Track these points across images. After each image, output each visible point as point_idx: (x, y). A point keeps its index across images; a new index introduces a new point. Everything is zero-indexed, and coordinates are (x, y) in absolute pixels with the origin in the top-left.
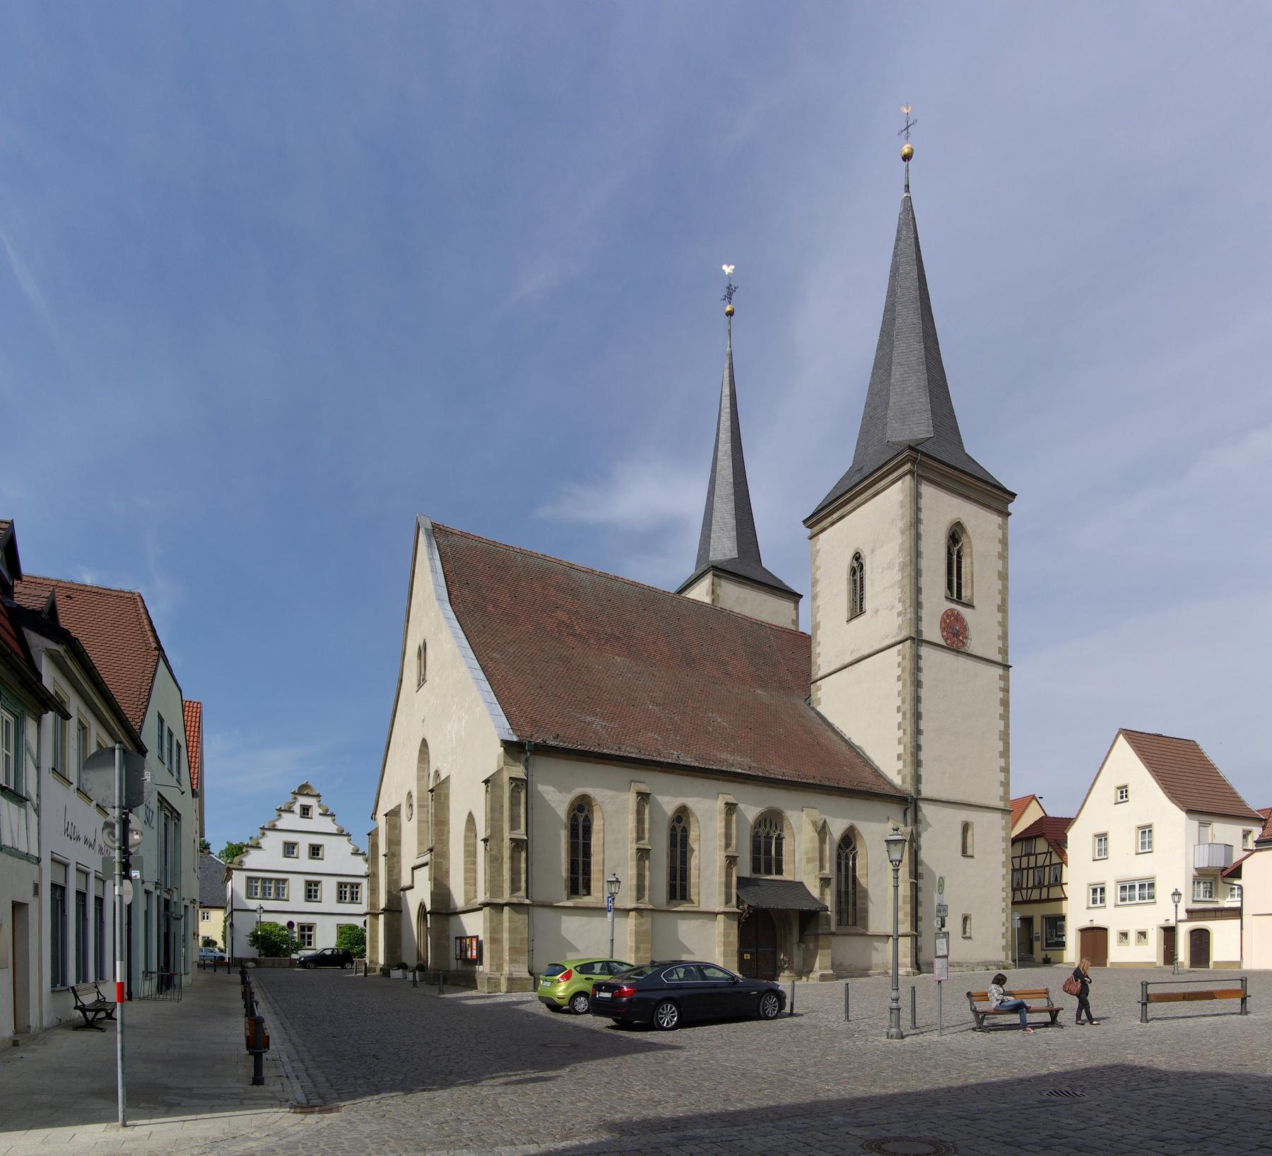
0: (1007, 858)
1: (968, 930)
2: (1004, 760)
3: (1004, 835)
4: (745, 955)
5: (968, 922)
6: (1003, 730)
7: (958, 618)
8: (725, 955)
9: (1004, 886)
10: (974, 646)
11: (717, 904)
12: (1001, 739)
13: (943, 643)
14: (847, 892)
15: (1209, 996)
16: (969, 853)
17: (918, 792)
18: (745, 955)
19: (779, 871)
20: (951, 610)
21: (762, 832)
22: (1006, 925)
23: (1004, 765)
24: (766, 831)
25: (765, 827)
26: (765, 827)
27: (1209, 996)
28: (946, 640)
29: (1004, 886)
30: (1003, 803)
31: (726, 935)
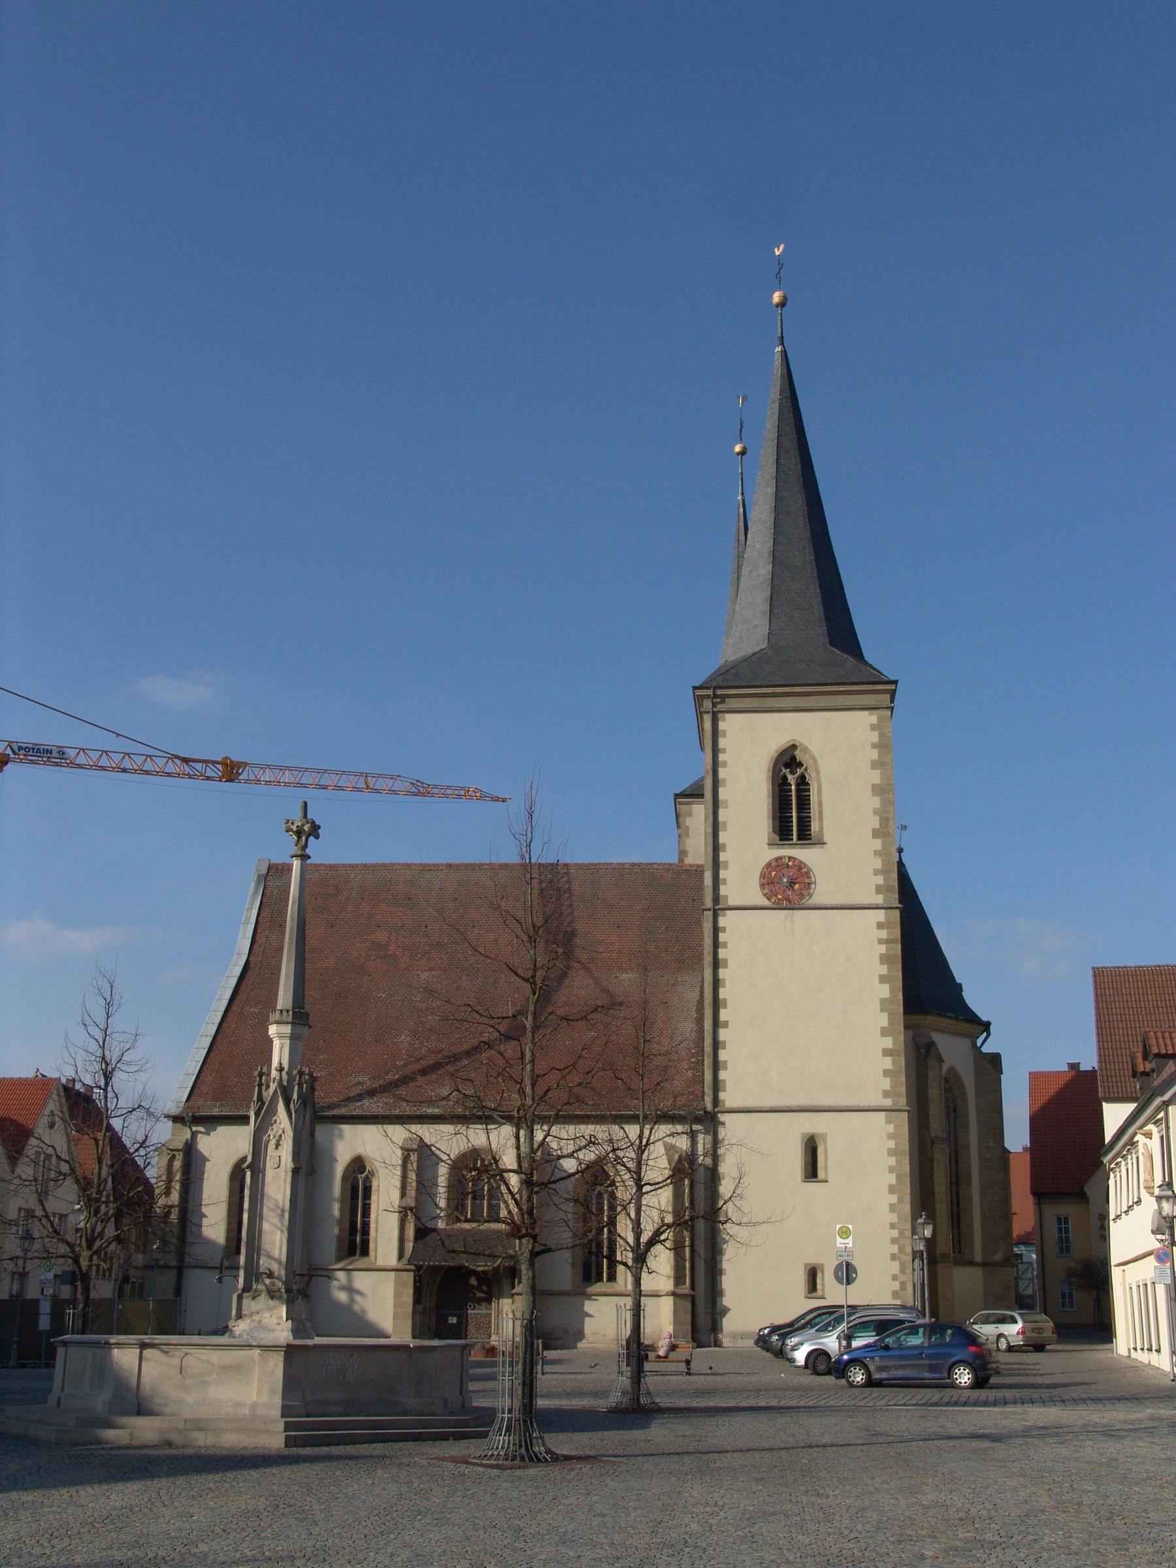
0: (898, 1178)
1: (819, 1287)
2: (891, 1038)
3: (894, 1147)
4: (450, 1318)
5: (819, 1275)
8: (396, 1316)
9: (896, 1221)
10: (822, 893)
11: (392, 1260)
13: (766, 903)
16: (821, 1174)
17: (716, 1101)
18: (450, 1318)
20: (778, 859)
22: (902, 1278)
23: (891, 1047)
28: (769, 899)
29: (896, 1221)
30: (891, 1100)
31: (397, 1295)
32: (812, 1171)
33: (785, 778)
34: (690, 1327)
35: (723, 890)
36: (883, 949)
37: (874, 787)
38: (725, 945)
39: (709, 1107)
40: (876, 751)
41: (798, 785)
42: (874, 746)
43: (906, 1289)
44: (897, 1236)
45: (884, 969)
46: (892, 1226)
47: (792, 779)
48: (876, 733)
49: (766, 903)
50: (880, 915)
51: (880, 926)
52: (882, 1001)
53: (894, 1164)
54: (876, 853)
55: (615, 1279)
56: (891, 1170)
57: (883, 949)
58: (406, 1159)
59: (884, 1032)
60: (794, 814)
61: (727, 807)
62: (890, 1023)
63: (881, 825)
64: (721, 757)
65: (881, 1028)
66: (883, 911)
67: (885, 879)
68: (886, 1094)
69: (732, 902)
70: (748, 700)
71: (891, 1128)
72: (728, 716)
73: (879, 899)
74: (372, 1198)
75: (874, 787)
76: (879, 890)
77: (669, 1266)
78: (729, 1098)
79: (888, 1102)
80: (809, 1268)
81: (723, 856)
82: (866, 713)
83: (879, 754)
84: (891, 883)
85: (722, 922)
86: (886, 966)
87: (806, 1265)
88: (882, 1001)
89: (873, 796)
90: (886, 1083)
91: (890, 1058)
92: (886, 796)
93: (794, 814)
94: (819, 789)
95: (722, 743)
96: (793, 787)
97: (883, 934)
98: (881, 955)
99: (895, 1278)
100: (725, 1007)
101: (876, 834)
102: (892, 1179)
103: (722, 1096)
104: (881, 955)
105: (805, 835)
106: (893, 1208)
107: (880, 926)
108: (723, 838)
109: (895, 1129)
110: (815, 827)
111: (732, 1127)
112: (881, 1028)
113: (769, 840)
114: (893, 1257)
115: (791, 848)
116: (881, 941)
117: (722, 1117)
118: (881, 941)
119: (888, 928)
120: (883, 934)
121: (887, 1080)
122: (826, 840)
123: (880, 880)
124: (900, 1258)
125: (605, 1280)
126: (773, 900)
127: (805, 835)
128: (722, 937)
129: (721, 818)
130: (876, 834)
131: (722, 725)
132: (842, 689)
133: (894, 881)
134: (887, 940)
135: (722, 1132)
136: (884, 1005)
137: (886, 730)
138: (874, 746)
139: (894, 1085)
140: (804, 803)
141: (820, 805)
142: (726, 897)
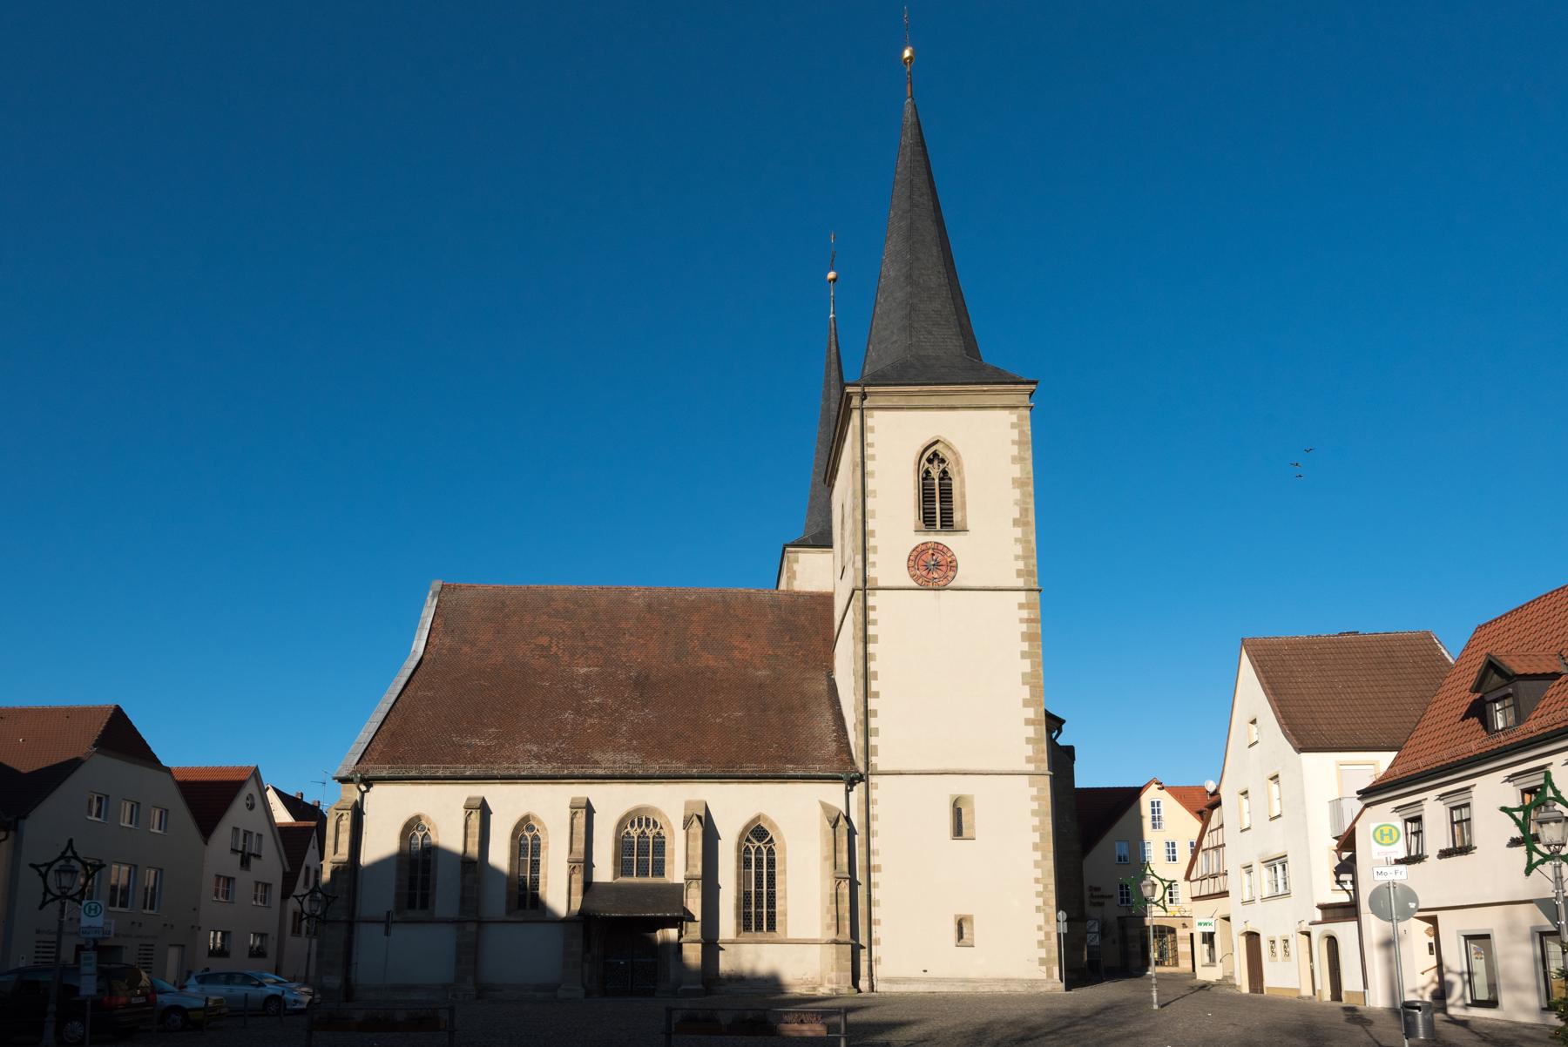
0: (1042, 837)
1: (965, 936)
2: (1032, 709)
6: (1029, 670)
7: (938, 548)
9: (1040, 876)
12: (1024, 684)
13: (914, 584)
14: (759, 895)
15: (1312, 971)
19: (662, 874)
21: (635, 832)
22: (1048, 929)
24: (639, 831)
25: (640, 825)
26: (640, 825)
27: (1312, 971)
29: (1040, 876)
30: (1033, 765)
32: (958, 831)
33: (927, 472)
34: (850, 973)
35: (871, 572)
36: (1024, 627)
37: (1015, 480)
38: (875, 622)
39: (862, 769)
40: (1016, 447)
41: (941, 479)
42: (1014, 442)
43: (1050, 939)
44: (1042, 890)
45: (1025, 646)
46: (1037, 881)
47: (935, 473)
48: (1016, 432)
49: (914, 584)
50: (1021, 597)
51: (1021, 606)
52: (1024, 675)
53: (1038, 824)
54: (1016, 540)
55: (774, 929)
56: (1035, 829)
57: (1024, 627)
58: (573, 816)
59: (1026, 704)
60: (938, 506)
61: (875, 497)
62: (1032, 695)
63: (1021, 515)
64: (868, 451)
65: (1023, 699)
66: (1024, 593)
67: (1026, 565)
68: (1029, 760)
69: (880, 584)
70: (895, 399)
71: (1034, 791)
72: (877, 413)
73: (1020, 583)
74: (541, 854)
75: (1015, 480)
76: (1019, 573)
77: (829, 916)
78: (879, 762)
79: (1031, 767)
80: (959, 918)
81: (871, 542)
82: (1006, 413)
83: (1019, 449)
84: (1031, 568)
85: (871, 601)
86: (1027, 643)
87: (956, 916)
88: (1024, 675)
89: (1014, 488)
90: (1029, 750)
91: (1032, 727)
92: (1025, 488)
93: (938, 506)
94: (962, 482)
95: (869, 438)
96: (937, 481)
97: (1025, 614)
98: (1023, 633)
99: (1040, 928)
100: (876, 679)
101: (1016, 523)
102: (1036, 838)
103: (873, 760)
104: (1023, 633)
105: (948, 523)
106: (1037, 864)
107: (1021, 606)
108: (871, 525)
109: (1038, 791)
110: (957, 517)
111: (882, 788)
112: (1023, 699)
113: (916, 527)
114: (1038, 909)
115: (937, 535)
116: (1022, 621)
117: (873, 779)
118: (1022, 621)
119: (1029, 608)
120: (1025, 614)
121: (1030, 747)
122: (968, 528)
123: (1021, 565)
124: (1044, 910)
125: (765, 929)
126: (920, 582)
127: (948, 523)
128: (872, 615)
129: (869, 506)
130: (1016, 523)
131: (869, 422)
132: (985, 389)
133: (1033, 566)
134: (1027, 619)
135: (874, 794)
136: (1026, 679)
137: (1025, 429)
138: (1014, 442)
139: (1036, 752)
140: (947, 495)
141: (963, 496)
142: (876, 579)
